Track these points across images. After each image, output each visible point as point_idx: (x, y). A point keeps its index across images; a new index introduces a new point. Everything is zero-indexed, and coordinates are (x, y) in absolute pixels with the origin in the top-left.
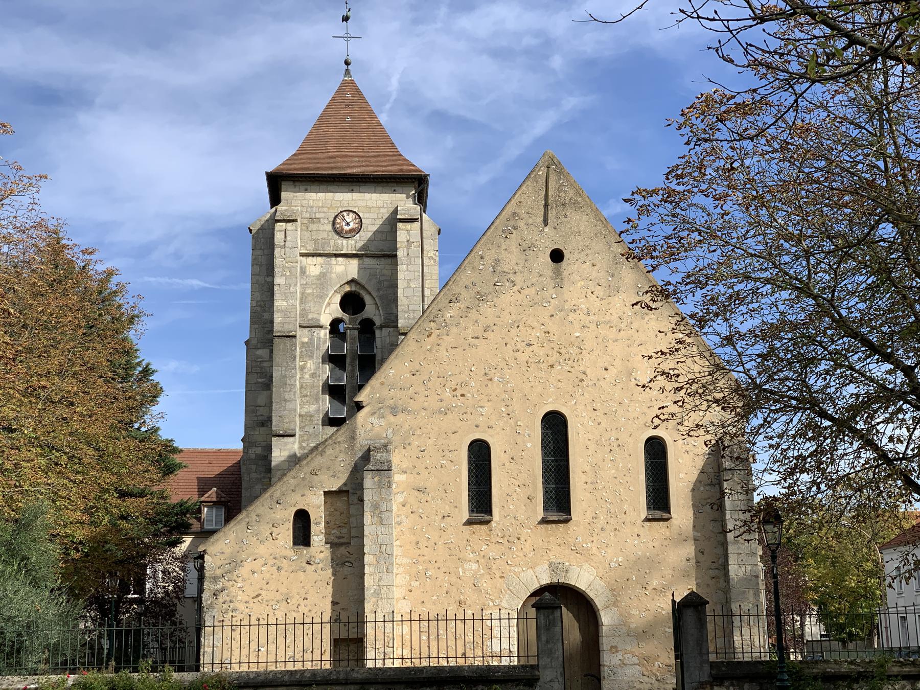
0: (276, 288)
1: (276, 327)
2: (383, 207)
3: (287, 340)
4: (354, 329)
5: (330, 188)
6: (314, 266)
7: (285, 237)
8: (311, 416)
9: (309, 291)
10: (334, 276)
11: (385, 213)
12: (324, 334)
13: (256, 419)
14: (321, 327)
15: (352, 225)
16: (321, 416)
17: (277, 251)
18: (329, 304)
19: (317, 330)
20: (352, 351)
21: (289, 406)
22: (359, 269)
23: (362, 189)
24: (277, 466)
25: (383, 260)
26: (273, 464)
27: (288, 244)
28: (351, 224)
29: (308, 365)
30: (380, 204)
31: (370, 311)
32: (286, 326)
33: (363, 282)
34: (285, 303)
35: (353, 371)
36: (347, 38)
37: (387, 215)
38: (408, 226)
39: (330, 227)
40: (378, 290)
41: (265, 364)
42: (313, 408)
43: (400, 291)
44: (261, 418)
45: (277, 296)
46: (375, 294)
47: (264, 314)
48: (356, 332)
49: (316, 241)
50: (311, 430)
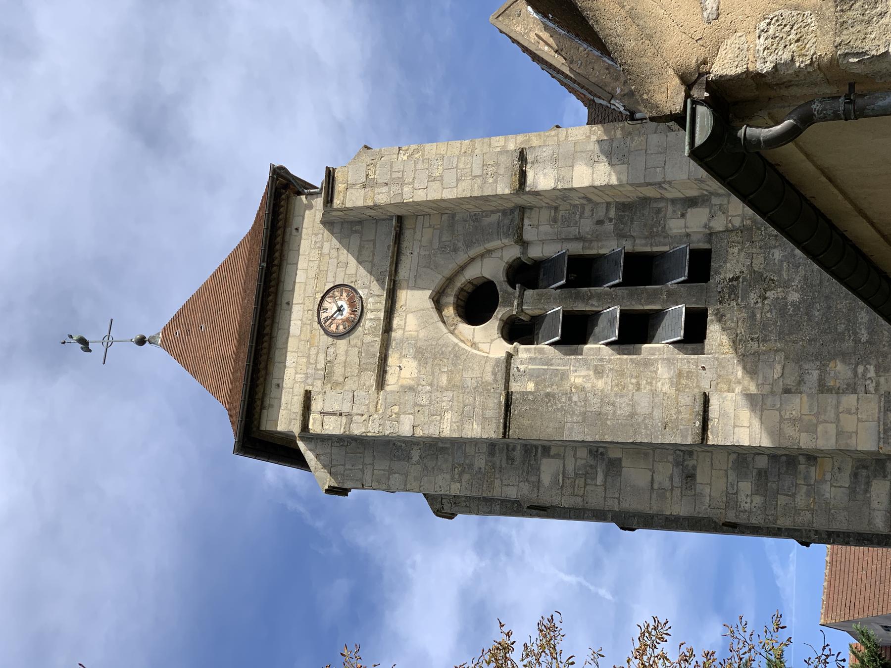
0: (419, 433)
1: (492, 432)
2: (321, 248)
3: (515, 410)
4: (521, 296)
5: (279, 343)
6: (403, 369)
7: (333, 414)
8: (680, 375)
9: (444, 380)
10: (422, 334)
11: (331, 243)
12: (524, 352)
13: (677, 492)
14: (510, 356)
15: (343, 303)
16: (682, 356)
17: (357, 430)
18: (474, 345)
19: (515, 363)
20: (559, 301)
21: (643, 407)
22: (416, 287)
23: (287, 286)
24: (771, 433)
25: (405, 244)
26: (766, 442)
27: (346, 409)
28: (340, 303)
29: (579, 381)
30: (315, 254)
31: (492, 269)
32: (489, 413)
33: (438, 279)
34: (448, 416)
35: (599, 297)
36: (108, 341)
37: (335, 241)
38: (339, 187)
39: (342, 343)
40: (455, 250)
41: (570, 468)
42: (663, 372)
43: (448, 195)
44: (677, 480)
45: (431, 431)
46: (462, 258)
47: (476, 467)
48: (529, 293)
49: (361, 369)
50: (709, 375)
